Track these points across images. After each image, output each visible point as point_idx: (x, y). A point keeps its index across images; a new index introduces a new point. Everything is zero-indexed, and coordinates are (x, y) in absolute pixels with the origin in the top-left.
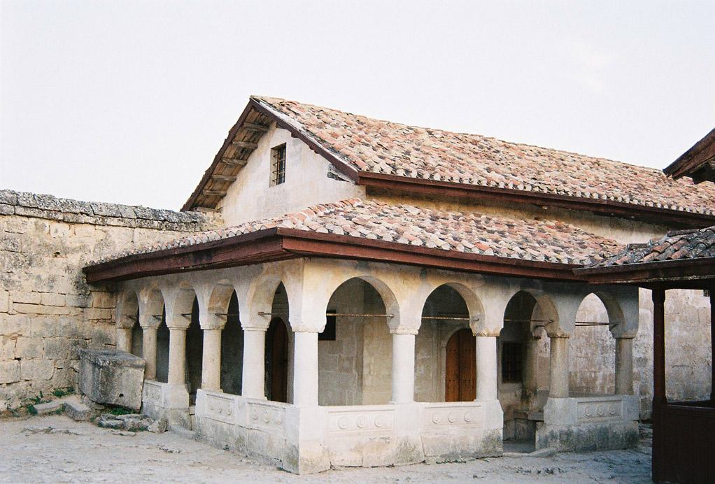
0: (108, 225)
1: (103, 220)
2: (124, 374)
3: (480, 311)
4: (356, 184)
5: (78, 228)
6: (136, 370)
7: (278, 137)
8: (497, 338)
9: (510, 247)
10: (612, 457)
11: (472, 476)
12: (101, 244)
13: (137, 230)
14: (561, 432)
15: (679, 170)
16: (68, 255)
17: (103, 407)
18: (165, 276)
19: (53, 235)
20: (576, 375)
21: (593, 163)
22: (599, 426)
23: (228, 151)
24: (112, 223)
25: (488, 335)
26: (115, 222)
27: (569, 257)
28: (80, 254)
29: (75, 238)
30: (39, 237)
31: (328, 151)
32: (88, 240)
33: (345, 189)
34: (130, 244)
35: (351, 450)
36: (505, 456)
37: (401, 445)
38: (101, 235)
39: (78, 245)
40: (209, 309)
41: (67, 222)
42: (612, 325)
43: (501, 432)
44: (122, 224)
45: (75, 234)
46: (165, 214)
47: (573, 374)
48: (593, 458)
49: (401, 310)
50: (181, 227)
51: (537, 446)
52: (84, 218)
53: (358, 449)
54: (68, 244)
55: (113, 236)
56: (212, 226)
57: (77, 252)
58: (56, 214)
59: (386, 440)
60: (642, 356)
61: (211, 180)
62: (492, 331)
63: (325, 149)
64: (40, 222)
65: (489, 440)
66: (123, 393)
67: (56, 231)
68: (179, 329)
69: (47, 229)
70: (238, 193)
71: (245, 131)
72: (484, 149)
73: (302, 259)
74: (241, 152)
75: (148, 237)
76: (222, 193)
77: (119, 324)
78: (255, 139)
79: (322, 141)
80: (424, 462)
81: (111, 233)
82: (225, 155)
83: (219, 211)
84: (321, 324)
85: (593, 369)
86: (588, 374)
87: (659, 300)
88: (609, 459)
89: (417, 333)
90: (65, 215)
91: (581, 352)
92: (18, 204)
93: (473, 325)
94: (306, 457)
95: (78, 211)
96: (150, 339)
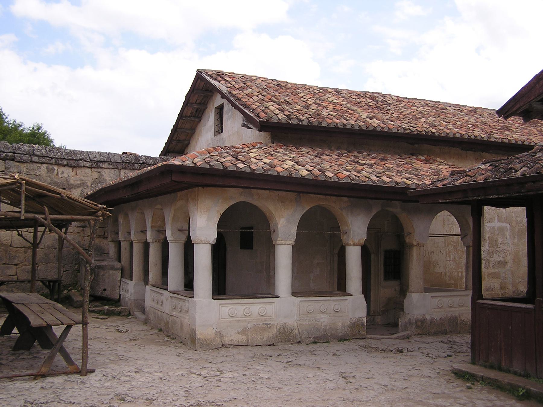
0: (101, 168)
1: (97, 164)
2: (107, 275)
3: (347, 226)
4: (260, 131)
5: (79, 171)
6: (115, 272)
8: (293, 246)
9: (368, 176)
10: (457, 339)
11: (332, 354)
12: (94, 182)
13: (122, 172)
14: (417, 320)
15: (508, 111)
16: (71, 190)
19: (60, 175)
20: (446, 275)
21: (470, 111)
22: (449, 315)
23: (185, 111)
24: (103, 166)
25: (354, 245)
26: (106, 165)
27: (417, 182)
28: (81, 189)
29: (77, 177)
30: (50, 177)
31: (241, 107)
32: (86, 178)
33: (252, 135)
35: (239, 332)
36: (368, 338)
37: (280, 329)
38: (95, 175)
39: (79, 182)
41: (71, 166)
42: (463, 236)
43: (365, 319)
44: (111, 166)
45: (76, 174)
46: (144, 158)
47: (443, 273)
48: (441, 340)
49: (279, 226)
51: (400, 329)
52: (82, 163)
53: (244, 331)
54: (72, 182)
55: (105, 175)
57: (78, 187)
58: (61, 161)
59: (268, 326)
60: (502, 259)
61: (176, 133)
62: (356, 241)
63: (239, 106)
64: (51, 167)
65: (355, 325)
66: (106, 288)
67: (63, 173)
68: (139, 242)
69: (56, 172)
70: (196, 142)
71: (196, 96)
72: (378, 102)
73: (197, 188)
74: (196, 112)
76: (187, 142)
77: (110, 239)
78: (205, 102)
79: (239, 100)
80: (300, 342)
81: (103, 173)
82: (184, 114)
84: (212, 236)
85: (460, 270)
86: (456, 274)
87: (478, 216)
88: (454, 341)
89: (294, 243)
90: (68, 161)
91: (450, 257)
92: (33, 154)
93: (343, 237)
94: (201, 337)
95: (78, 158)
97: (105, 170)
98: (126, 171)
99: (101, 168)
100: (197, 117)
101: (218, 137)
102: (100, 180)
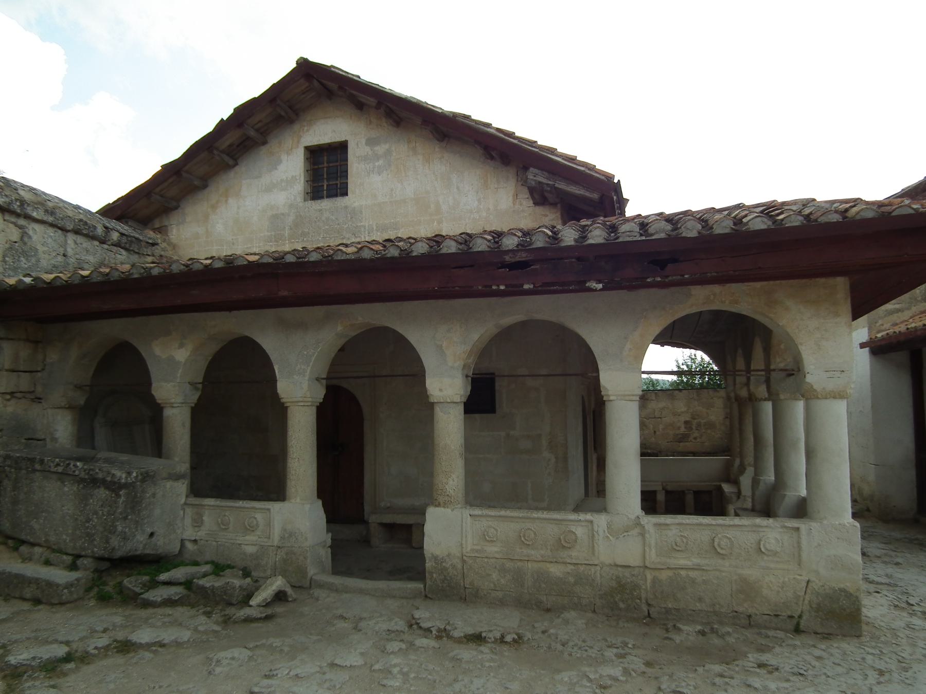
6: (176, 484)
7: (324, 130)
13: (71, 238)
17: (106, 565)
24: (35, 214)
34: (60, 259)
55: (35, 238)
70: (214, 207)
75: (87, 251)
76: (175, 204)
81: (31, 233)
83: (162, 230)
96: (183, 425)
97: (37, 227)
98: (80, 239)
99: (28, 217)
100: (232, 157)
101: (326, 204)
102: (25, 248)
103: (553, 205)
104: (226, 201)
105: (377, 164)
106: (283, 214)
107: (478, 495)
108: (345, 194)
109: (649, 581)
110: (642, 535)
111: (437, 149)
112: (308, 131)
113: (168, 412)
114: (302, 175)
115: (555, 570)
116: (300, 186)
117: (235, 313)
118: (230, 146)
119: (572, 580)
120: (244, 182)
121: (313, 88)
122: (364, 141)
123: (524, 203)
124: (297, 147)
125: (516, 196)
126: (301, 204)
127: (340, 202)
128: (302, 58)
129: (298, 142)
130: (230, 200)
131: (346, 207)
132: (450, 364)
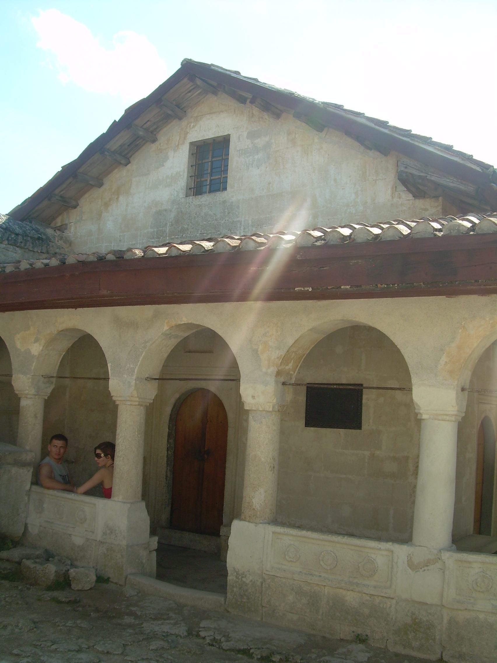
18: (108, 311)
40: (278, 374)
50: (26, 241)
56: (59, 247)
68: (140, 405)
70: (107, 205)
83: (62, 228)
101: (205, 199)
103: (436, 197)
104: (117, 199)
105: (256, 157)
106: (166, 210)
107: (288, 513)
108: (225, 189)
109: (445, 621)
110: (443, 570)
111: (316, 140)
112: (194, 127)
113: (24, 403)
114: (186, 170)
115: (351, 598)
116: (182, 183)
117: (79, 309)
118: (121, 146)
119: (366, 611)
120: (134, 179)
121: (196, 84)
122: (245, 134)
123: (403, 195)
124: (183, 143)
125: (395, 188)
126: (183, 200)
127: (220, 196)
128: (185, 60)
129: (185, 138)
130: (121, 198)
131: (224, 202)
132: (264, 370)
